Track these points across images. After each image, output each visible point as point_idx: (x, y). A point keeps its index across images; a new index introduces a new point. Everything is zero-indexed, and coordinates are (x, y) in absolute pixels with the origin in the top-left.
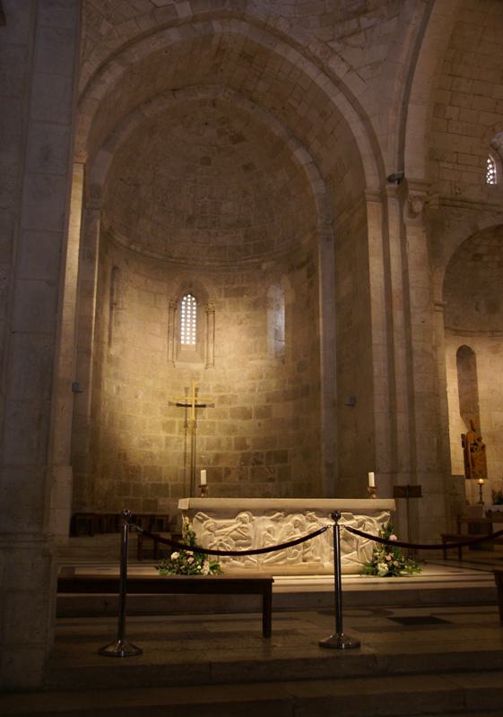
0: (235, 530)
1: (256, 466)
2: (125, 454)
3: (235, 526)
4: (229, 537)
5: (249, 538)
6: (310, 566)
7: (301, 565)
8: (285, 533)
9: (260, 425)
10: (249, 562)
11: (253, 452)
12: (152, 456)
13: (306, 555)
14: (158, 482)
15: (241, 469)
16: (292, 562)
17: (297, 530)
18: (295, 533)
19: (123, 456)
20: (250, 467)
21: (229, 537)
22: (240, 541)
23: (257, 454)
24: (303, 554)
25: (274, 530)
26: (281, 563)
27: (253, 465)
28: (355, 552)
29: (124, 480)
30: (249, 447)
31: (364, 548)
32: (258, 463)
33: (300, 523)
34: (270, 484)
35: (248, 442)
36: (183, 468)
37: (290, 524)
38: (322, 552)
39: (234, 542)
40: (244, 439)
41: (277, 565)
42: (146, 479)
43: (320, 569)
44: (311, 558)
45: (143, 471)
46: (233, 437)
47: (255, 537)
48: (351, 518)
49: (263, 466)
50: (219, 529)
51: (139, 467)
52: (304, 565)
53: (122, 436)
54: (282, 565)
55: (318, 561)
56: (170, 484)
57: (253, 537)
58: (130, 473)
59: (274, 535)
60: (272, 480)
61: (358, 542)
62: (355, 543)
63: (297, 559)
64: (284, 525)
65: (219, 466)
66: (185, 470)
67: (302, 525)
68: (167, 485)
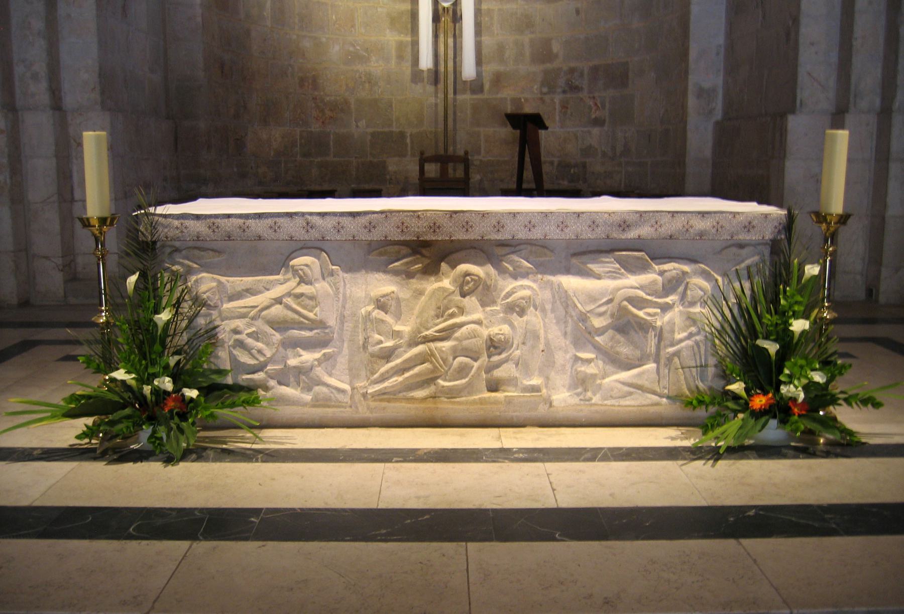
0: (278, 301)
1: (568, 96)
2: (315, 80)
3: (277, 291)
4: (259, 323)
5: (320, 324)
6: (509, 401)
7: (482, 401)
8: (433, 313)
9: (578, 12)
10: (324, 389)
11: (565, 68)
12: (370, 80)
13: (498, 373)
14: (386, 130)
15: (541, 99)
16: (452, 393)
17: (471, 302)
18: (462, 311)
19: (309, 81)
20: (558, 98)
21: (260, 325)
22: (295, 333)
23: (572, 71)
24: (489, 370)
25: (398, 300)
26: (420, 393)
27: (564, 92)
28: (651, 366)
29: (315, 128)
30: (556, 56)
31: (677, 354)
32: (574, 88)
33: (478, 281)
34: (596, 131)
35: (556, 47)
36: (432, 100)
37: (446, 283)
38: (549, 363)
39: (277, 337)
40: (547, 42)
41: (413, 399)
42: (363, 123)
43: (542, 411)
44: (512, 382)
45: (352, 106)
46: (526, 38)
47: (342, 319)
48: (643, 268)
49: (584, 94)
50: (231, 298)
51: (346, 102)
52: (496, 402)
53: (307, 44)
54: (424, 399)
55: (535, 389)
56: (409, 131)
57: (332, 322)
58: (328, 113)
59: (398, 317)
60: (598, 122)
61: (660, 336)
62: (652, 342)
63: (469, 385)
64: (431, 285)
65: (499, 96)
66: (436, 105)
67: (487, 288)
68: (402, 135)
